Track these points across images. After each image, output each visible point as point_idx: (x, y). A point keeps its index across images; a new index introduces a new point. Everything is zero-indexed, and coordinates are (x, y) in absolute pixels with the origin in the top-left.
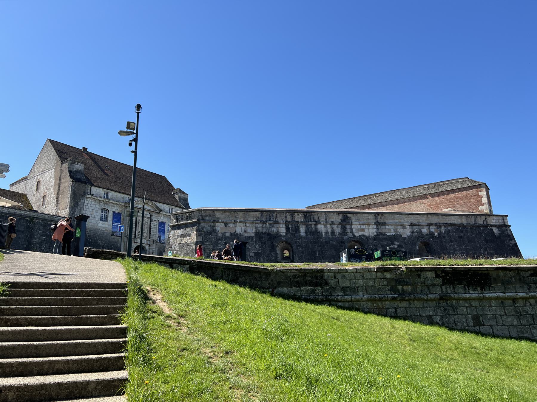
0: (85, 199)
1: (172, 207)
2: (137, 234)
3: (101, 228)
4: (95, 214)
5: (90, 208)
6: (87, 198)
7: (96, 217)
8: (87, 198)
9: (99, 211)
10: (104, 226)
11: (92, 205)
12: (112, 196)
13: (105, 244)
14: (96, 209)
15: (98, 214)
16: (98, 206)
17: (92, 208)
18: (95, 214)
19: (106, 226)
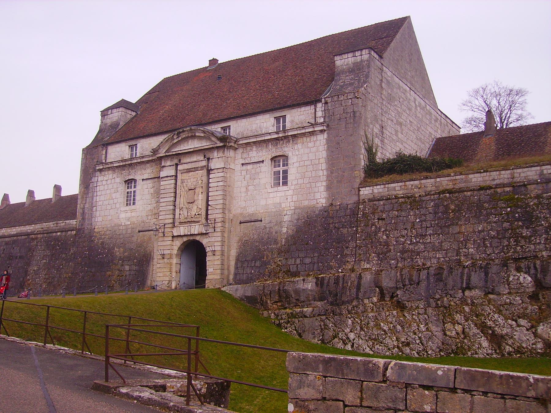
0: (98, 173)
1: (278, 114)
2: (177, 216)
3: (124, 222)
4: (114, 196)
5: (106, 187)
6: (100, 170)
7: (116, 201)
8: (100, 170)
9: (122, 188)
10: (129, 215)
11: (109, 182)
12: (142, 147)
13: (124, 252)
14: (115, 186)
15: (118, 195)
16: (118, 180)
17: (110, 186)
18: (114, 196)
19: (133, 214)
